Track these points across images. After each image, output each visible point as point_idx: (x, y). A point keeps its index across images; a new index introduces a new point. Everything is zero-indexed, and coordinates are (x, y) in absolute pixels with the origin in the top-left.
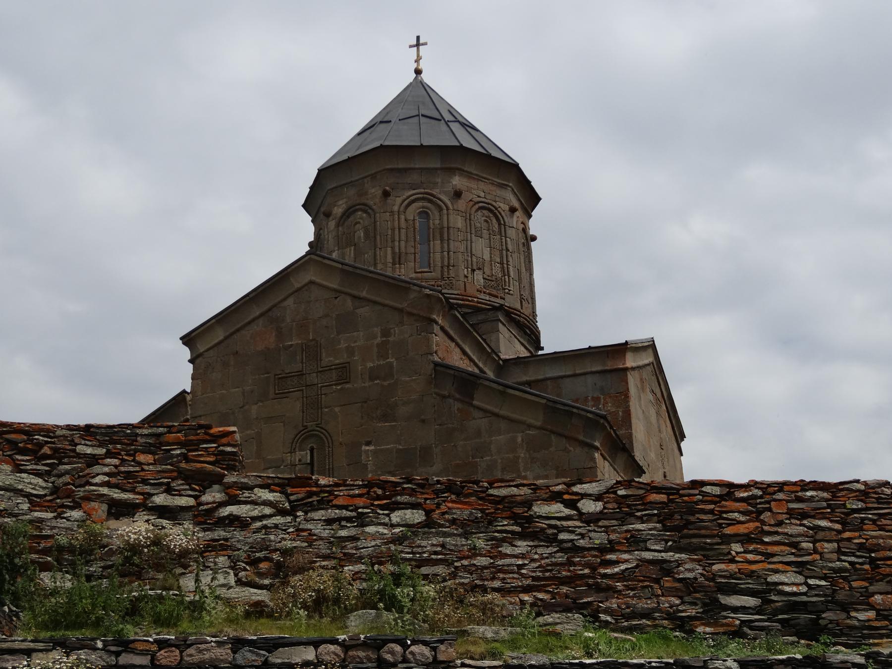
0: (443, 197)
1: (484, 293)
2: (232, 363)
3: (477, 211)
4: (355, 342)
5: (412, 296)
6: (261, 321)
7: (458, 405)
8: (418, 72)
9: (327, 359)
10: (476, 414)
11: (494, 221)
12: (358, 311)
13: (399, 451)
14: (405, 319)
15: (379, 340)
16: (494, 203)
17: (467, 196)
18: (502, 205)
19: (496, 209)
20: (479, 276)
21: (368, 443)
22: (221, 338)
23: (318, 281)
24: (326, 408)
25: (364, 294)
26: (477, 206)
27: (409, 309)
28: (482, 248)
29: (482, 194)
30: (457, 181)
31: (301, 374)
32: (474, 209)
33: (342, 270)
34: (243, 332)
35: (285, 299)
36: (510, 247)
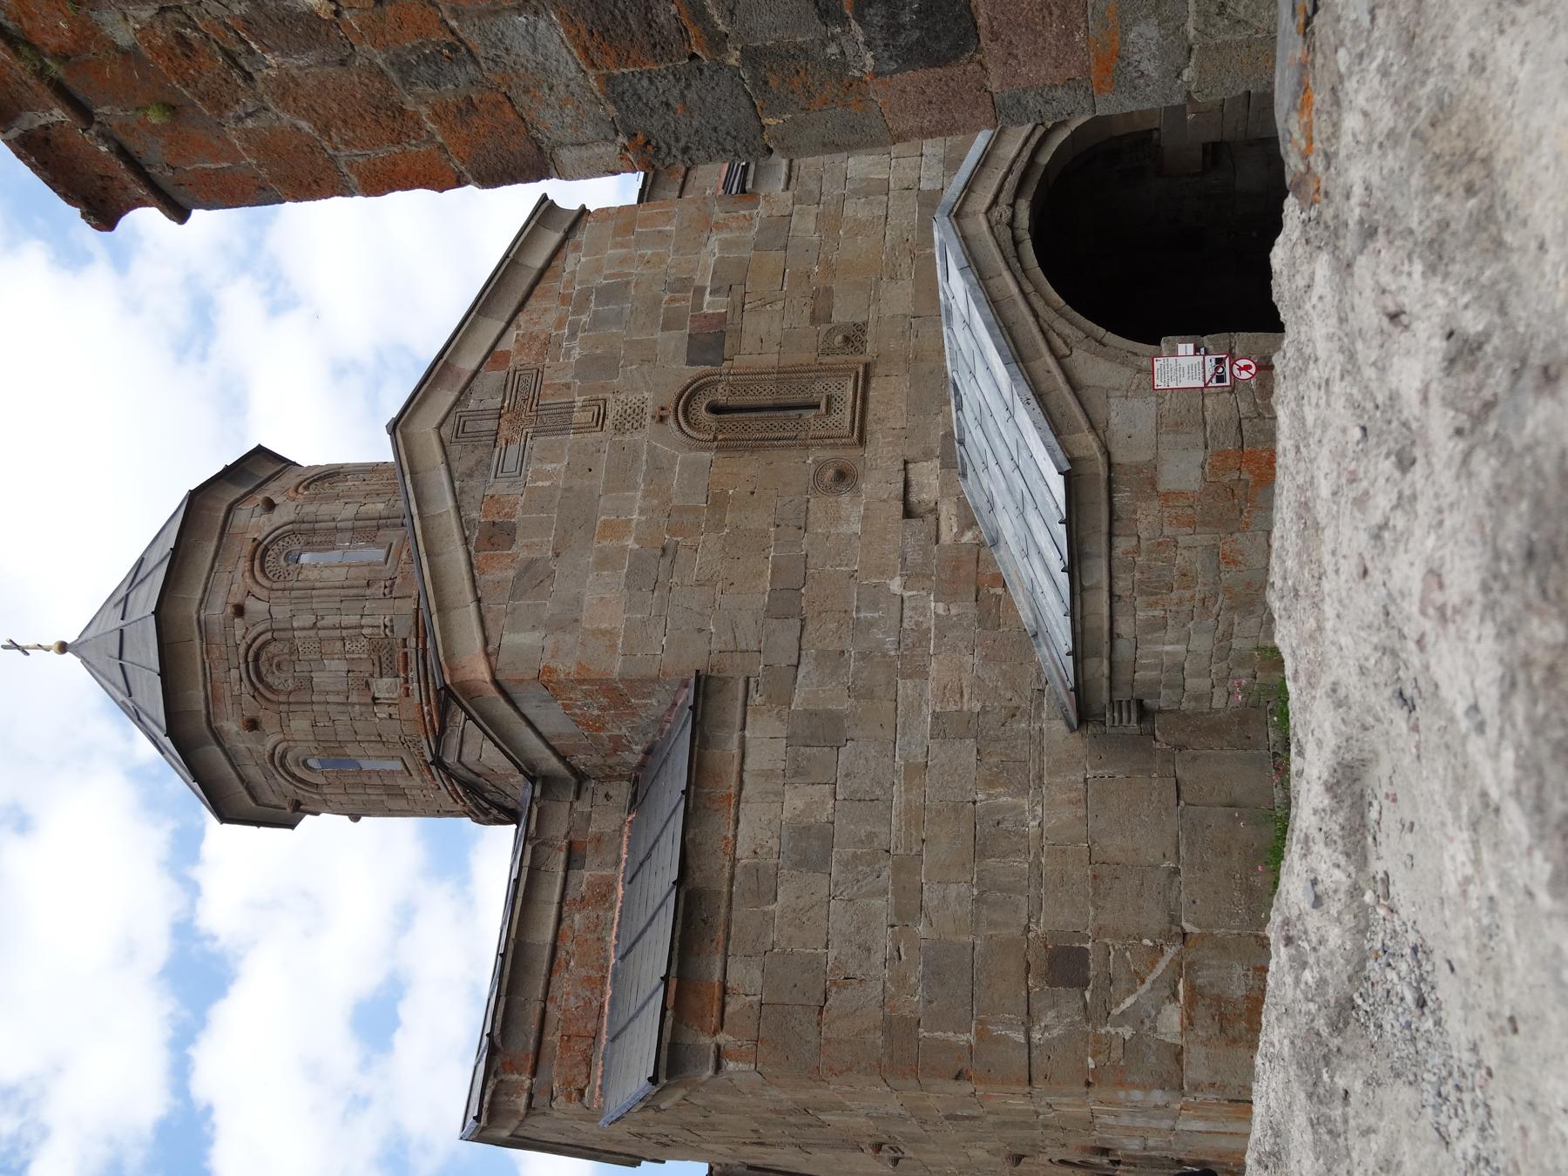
0: (269, 746)
1: (406, 681)
3: (269, 687)
8: (63, 648)
11: (271, 648)
16: (242, 650)
17: (251, 708)
18: (239, 633)
19: (250, 646)
20: (384, 687)
26: (259, 686)
28: (331, 673)
29: (234, 673)
30: (231, 726)
32: (269, 695)
36: (308, 620)
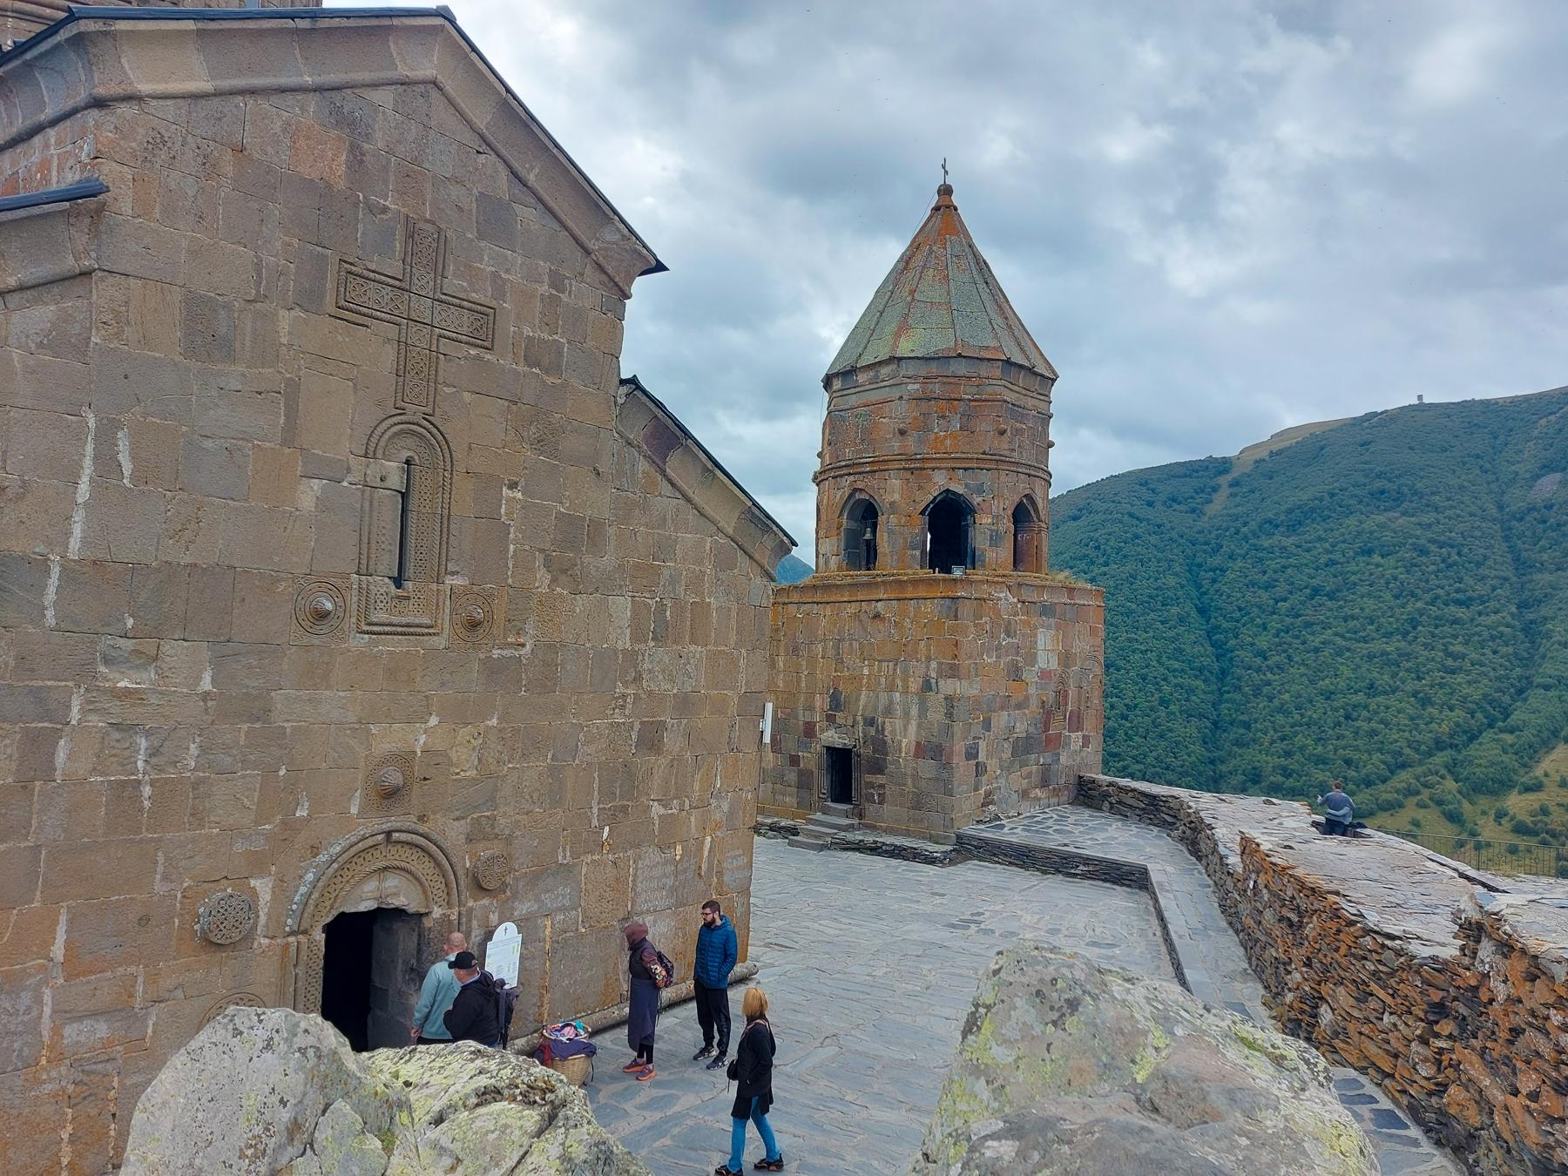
2: (229, 170)
4: (507, 271)
5: (610, 236)
6: (312, 102)
7: (643, 466)
9: (455, 283)
10: (666, 488)
12: (518, 208)
13: (560, 517)
14: (589, 270)
15: (544, 289)
21: (513, 486)
22: (206, 86)
23: (448, 89)
24: (448, 386)
25: (531, 178)
27: (601, 261)
31: (401, 287)
33: (505, 103)
34: (264, 104)
35: (375, 85)
